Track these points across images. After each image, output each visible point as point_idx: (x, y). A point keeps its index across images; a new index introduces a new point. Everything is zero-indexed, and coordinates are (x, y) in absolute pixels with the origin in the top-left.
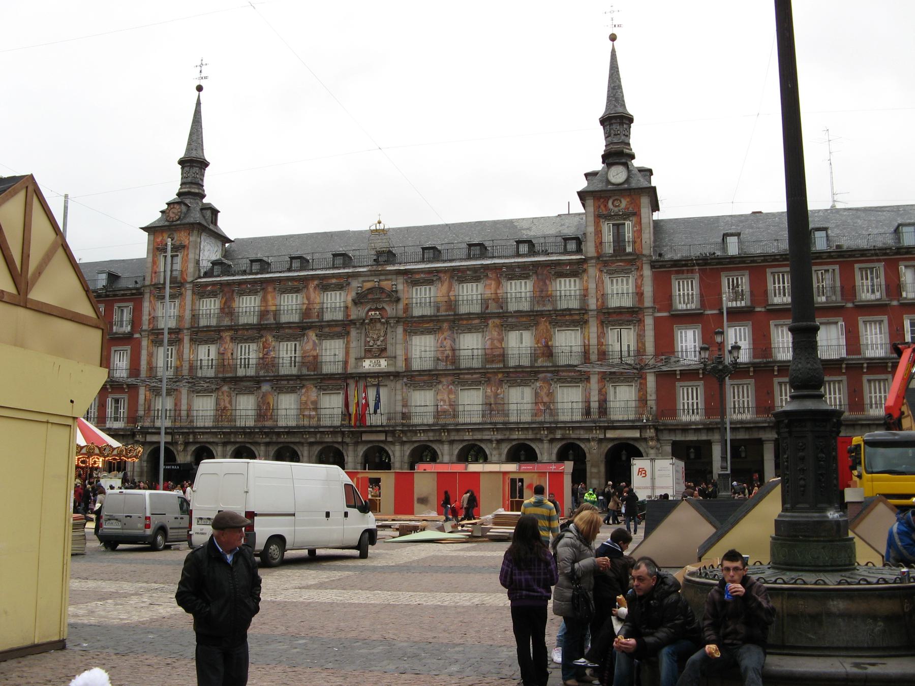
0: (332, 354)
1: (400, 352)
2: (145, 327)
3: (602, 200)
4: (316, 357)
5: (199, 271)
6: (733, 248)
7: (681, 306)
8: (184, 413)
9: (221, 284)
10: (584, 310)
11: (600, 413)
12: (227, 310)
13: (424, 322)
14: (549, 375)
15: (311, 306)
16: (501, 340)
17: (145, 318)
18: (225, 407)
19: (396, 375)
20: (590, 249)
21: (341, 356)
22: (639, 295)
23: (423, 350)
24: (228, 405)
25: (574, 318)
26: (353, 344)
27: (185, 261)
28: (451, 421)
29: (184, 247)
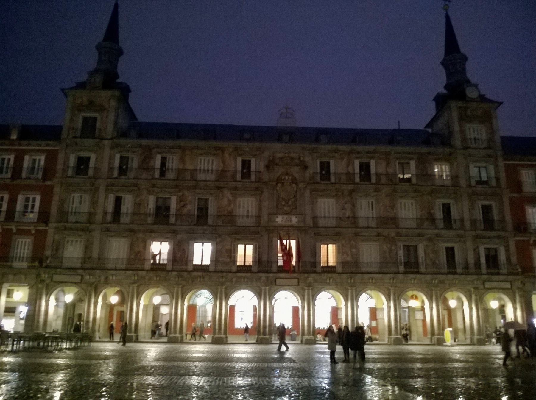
4: (231, 212)
8: (95, 255)
15: (226, 169)
16: (393, 207)
17: (59, 167)
21: (253, 211)
24: (142, 250)
26: (265, 204)
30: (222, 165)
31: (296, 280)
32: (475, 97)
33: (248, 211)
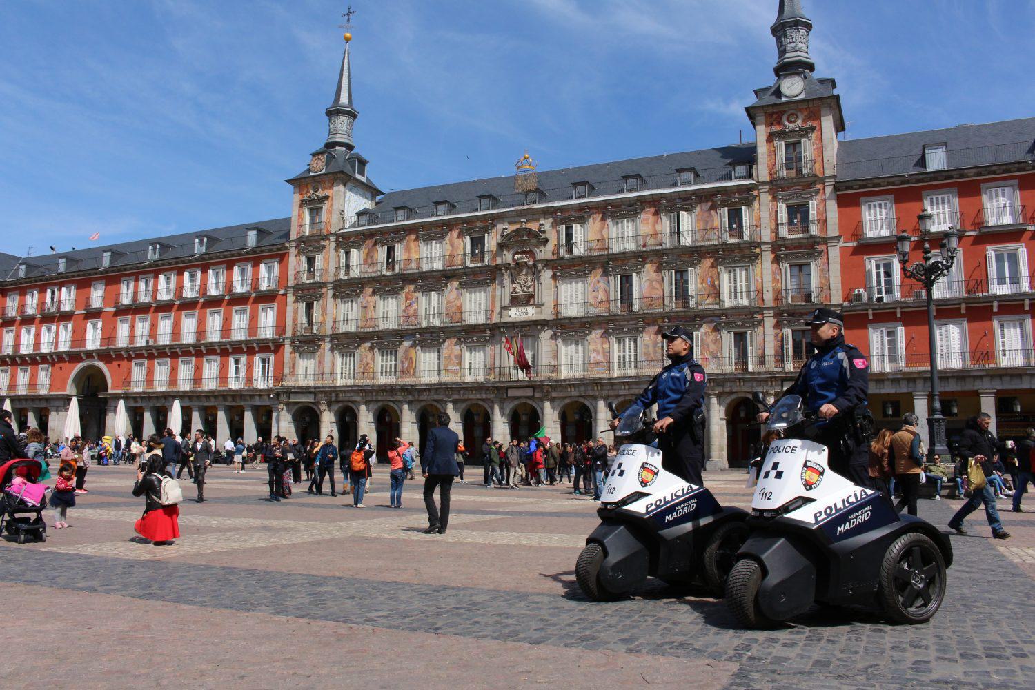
0: (475, 306)
2: (291, 282)
3: (775, 116)
5: (343, 221)
6: (937, 161)
8: (327, 370)
9: (362, 232)
11: (777, 361)
13: (573, 266)
14: (715, 319)
17: (291, 273)
19: (544, 324)
20: (762, 171)
23: (574, 297)
27: (330, 212)
28: (603, 374)
29: (327, 198)
30: (451, 248)
32: (797, 92)
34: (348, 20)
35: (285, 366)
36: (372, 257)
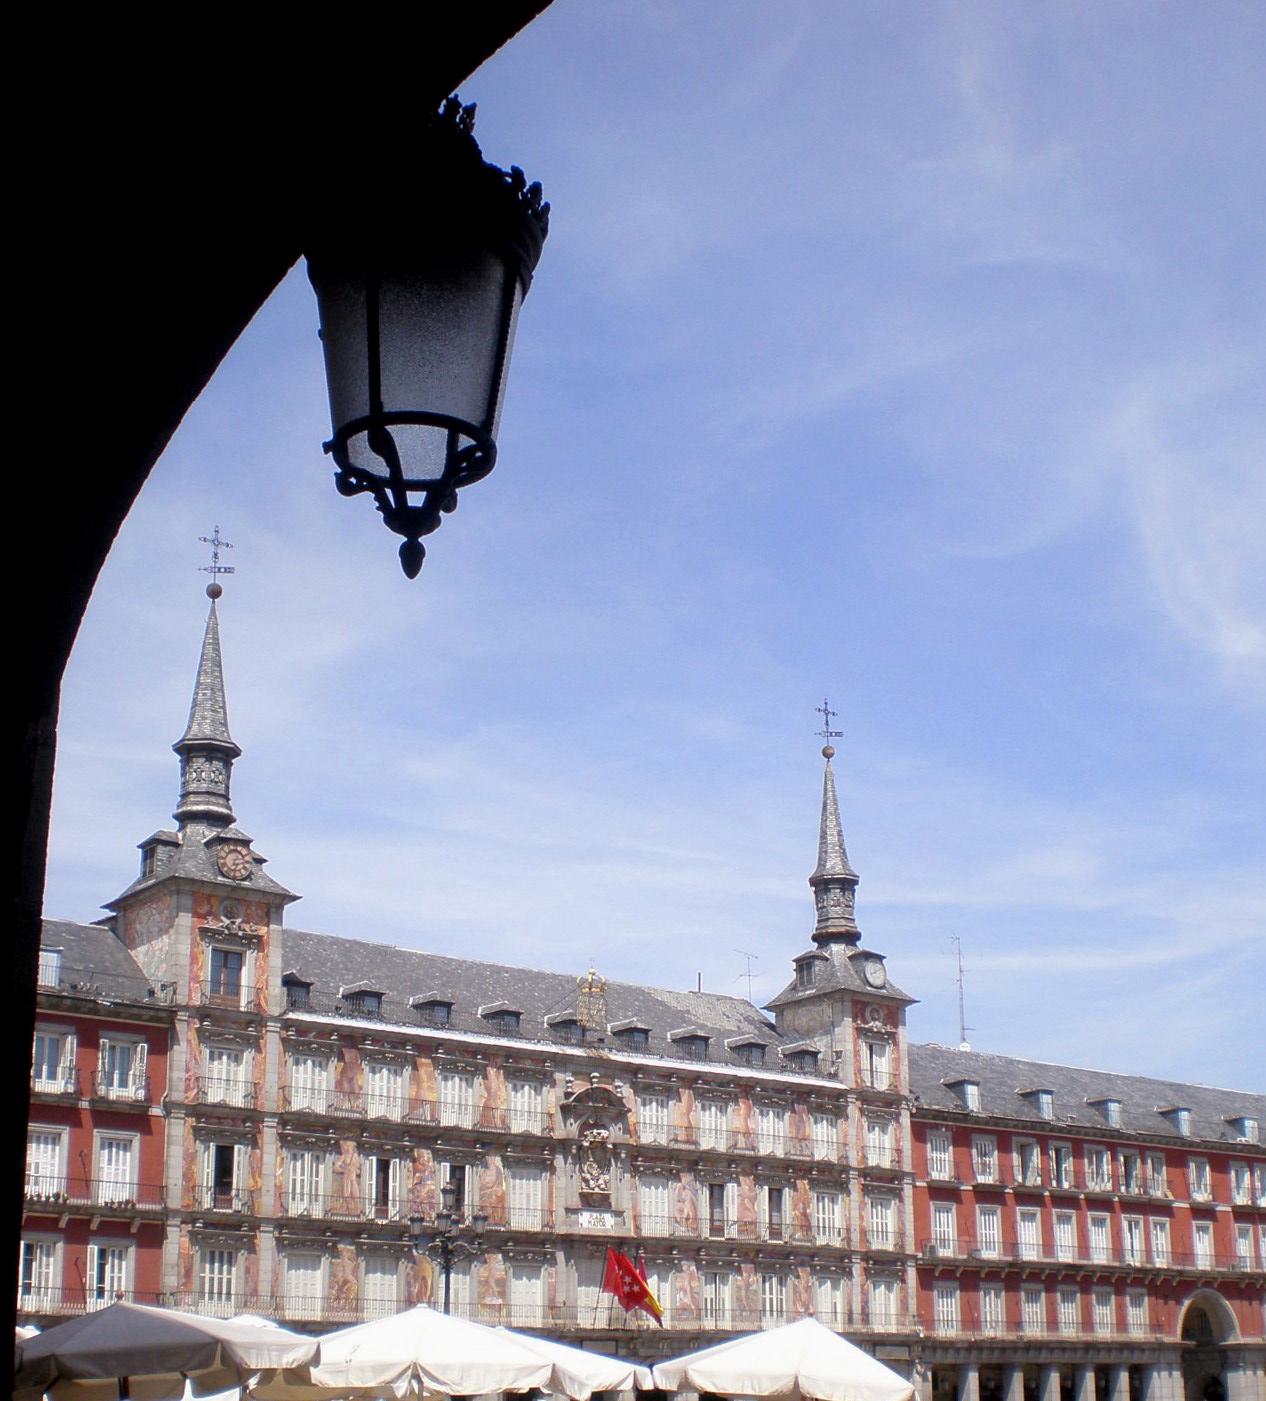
1: (626, 1205)
3: (859, 1006)
7: (935, 1175)
10: (846, 1169)
12: (346, 1085)
16: (753, 1199)
18: (346, 1282)
22: (899, 1151)
24: (351, 1278)
25: (830, 1178)
31: (614, 1343)
33: (528, 1196)
34: (216, 555)
35: (165, 1269)
36: (351, 1080)
